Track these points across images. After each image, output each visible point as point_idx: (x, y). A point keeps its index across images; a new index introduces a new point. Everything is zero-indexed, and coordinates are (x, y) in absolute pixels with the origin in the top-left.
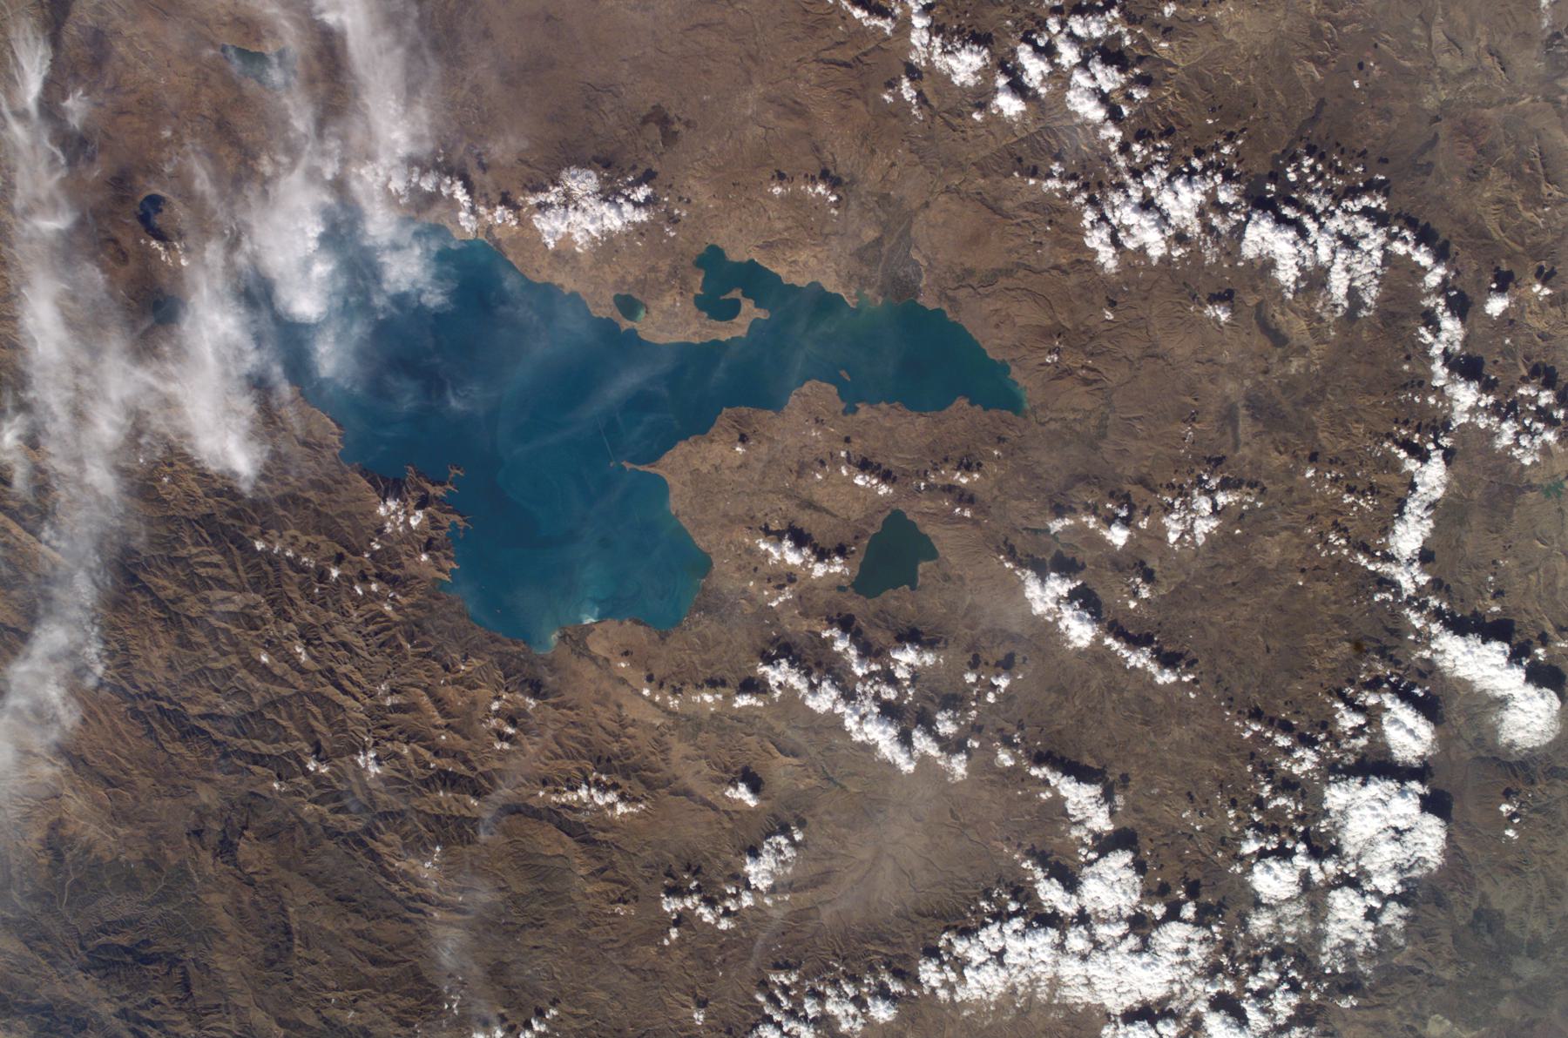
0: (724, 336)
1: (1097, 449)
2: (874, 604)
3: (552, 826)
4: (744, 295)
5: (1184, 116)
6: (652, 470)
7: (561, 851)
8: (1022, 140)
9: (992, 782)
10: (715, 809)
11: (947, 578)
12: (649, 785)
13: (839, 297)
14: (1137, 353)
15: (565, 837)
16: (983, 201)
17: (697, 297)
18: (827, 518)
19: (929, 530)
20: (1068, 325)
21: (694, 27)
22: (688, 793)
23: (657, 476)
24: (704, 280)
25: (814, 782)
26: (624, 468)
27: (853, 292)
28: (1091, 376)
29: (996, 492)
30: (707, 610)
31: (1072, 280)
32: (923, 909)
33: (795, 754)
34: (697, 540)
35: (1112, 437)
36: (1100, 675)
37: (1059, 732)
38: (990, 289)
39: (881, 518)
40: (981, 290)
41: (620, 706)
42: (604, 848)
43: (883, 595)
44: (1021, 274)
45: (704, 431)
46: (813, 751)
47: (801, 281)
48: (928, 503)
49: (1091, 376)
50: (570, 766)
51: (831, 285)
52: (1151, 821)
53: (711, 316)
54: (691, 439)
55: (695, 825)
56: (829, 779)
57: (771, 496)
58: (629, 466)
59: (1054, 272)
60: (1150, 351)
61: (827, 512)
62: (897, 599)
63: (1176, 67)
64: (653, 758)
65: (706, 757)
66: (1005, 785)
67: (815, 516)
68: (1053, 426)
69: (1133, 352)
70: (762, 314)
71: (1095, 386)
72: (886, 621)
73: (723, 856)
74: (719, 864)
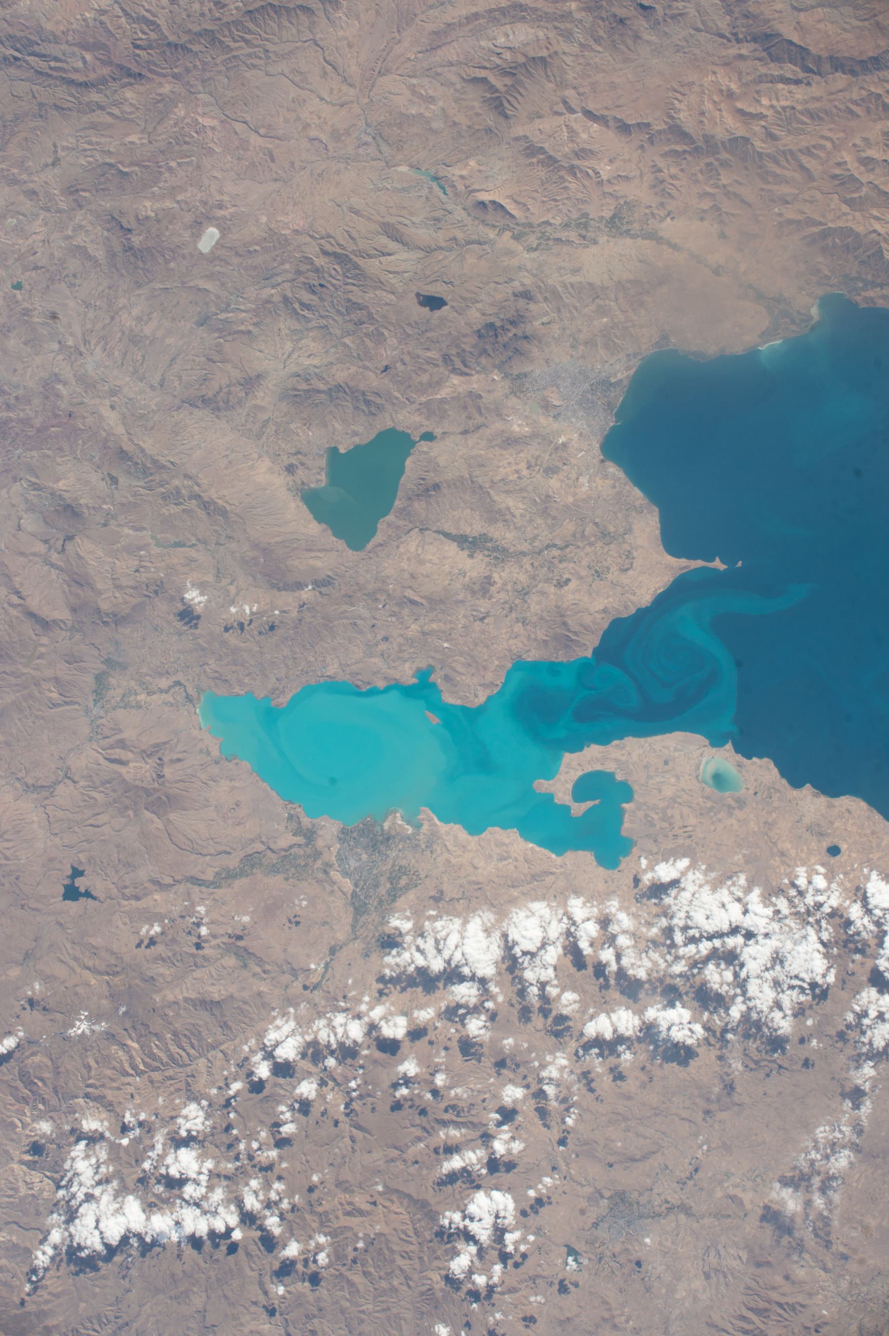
0: (594, 751)
1: (108, 662)
2: (385, 422)
3: (813, 50)
4: (568, 808)
5: (10, 1099)
6: (684, 562)
7: (802, 16)
8: (214, 1048)
9: (221, 206)
10: (589, 114)
11: (290, 469)
12: (677, 132)
13: (445, 820)
14: (61, 789)
15: (795, 39)
16: (260, 962)
17: (629, 798)
18: (448, 527)
19: (314, 528)
20: (148, 814)
21: (645, 1157)
22: (624, 128)
23: (676, 554)
24: (621, 822)
25: (457, 171)
26: (722, 561)
27: (425, 828)
28: (118, 753)
29: (232, 589)
30: (606, 384)
31: (143, 874)
32: (303, 18)
33: (482, 204)
34: (621, 475)
35: (89, 679)
36: (90, 368)
37: (139, 285)
38: (249, 851)
39: (379, 538)
40: (261, 847)
41: (723, 236)
42: (742, 32)
43: (372, 436)
44: (209, 876)
45: (617, 623)
46: (459, 214)
47: (495, 834)
48: (318, 564)
49: (118, 753)
50: (788, 141)
51: (454, 833)
52: (14, 181)
53: (611, 776)
54: (633, 611)
55: (613, 86)
56: (436, 179)
57: (525, 547)
58: (718, 564)
59: (168, 880)
60: (44, 794)
61: (447, 535)
62: (356, 434)
63: (21, 1162)
64: (674, 170)
65: (601, 183)
66: (205, 203)
67: (467, 530)
68: (164, 683)
69: (64, 791)
70: (543, 785)
71: (111, 741)
72: (367, 403)
73: (576, 49)
74: (579, 36)
